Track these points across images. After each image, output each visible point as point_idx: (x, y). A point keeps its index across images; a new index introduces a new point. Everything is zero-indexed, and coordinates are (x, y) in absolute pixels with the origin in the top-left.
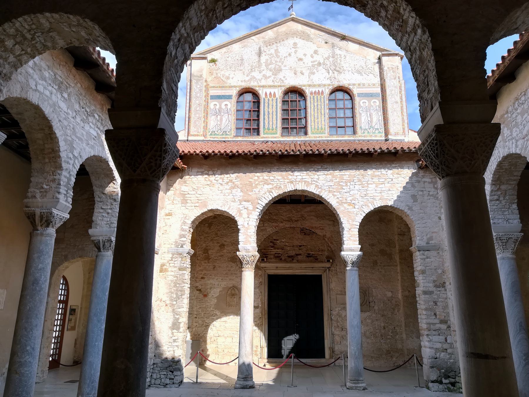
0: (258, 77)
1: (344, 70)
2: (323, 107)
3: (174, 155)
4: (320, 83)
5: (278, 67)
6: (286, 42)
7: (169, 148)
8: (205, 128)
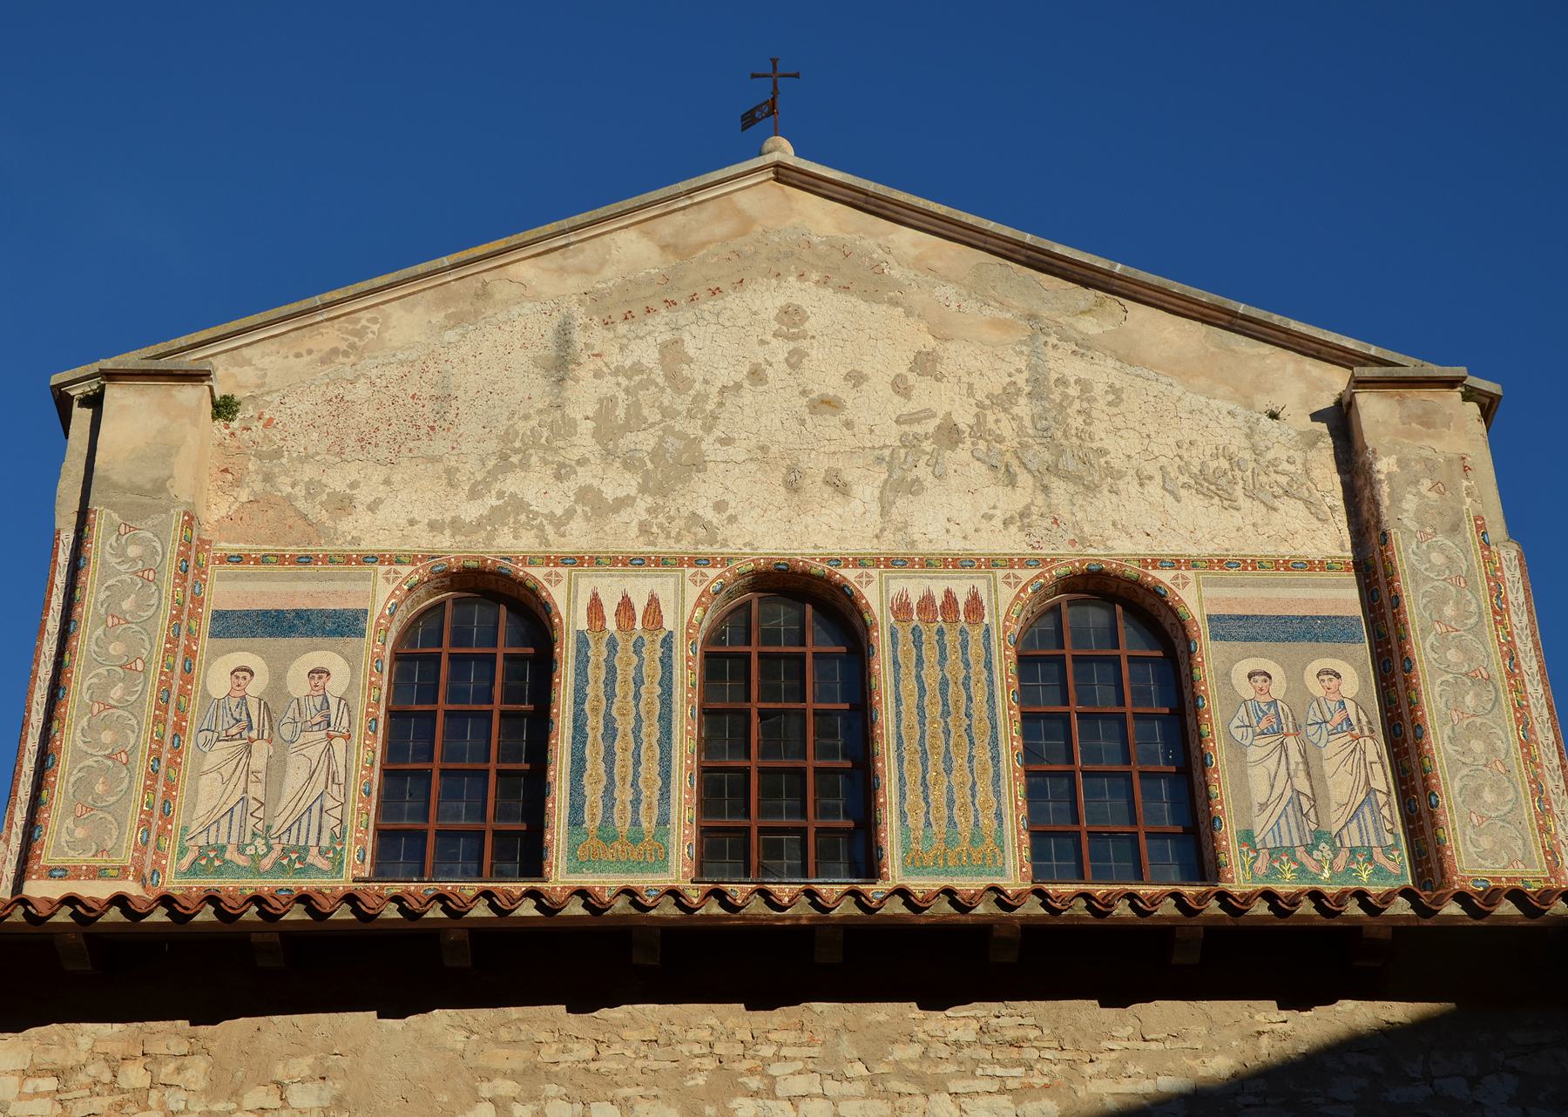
1: (1114, 474)
2: (979, 696)
4: (957, 546)
5: (680, 444)
6: (733, 302)
8: (156, 822)
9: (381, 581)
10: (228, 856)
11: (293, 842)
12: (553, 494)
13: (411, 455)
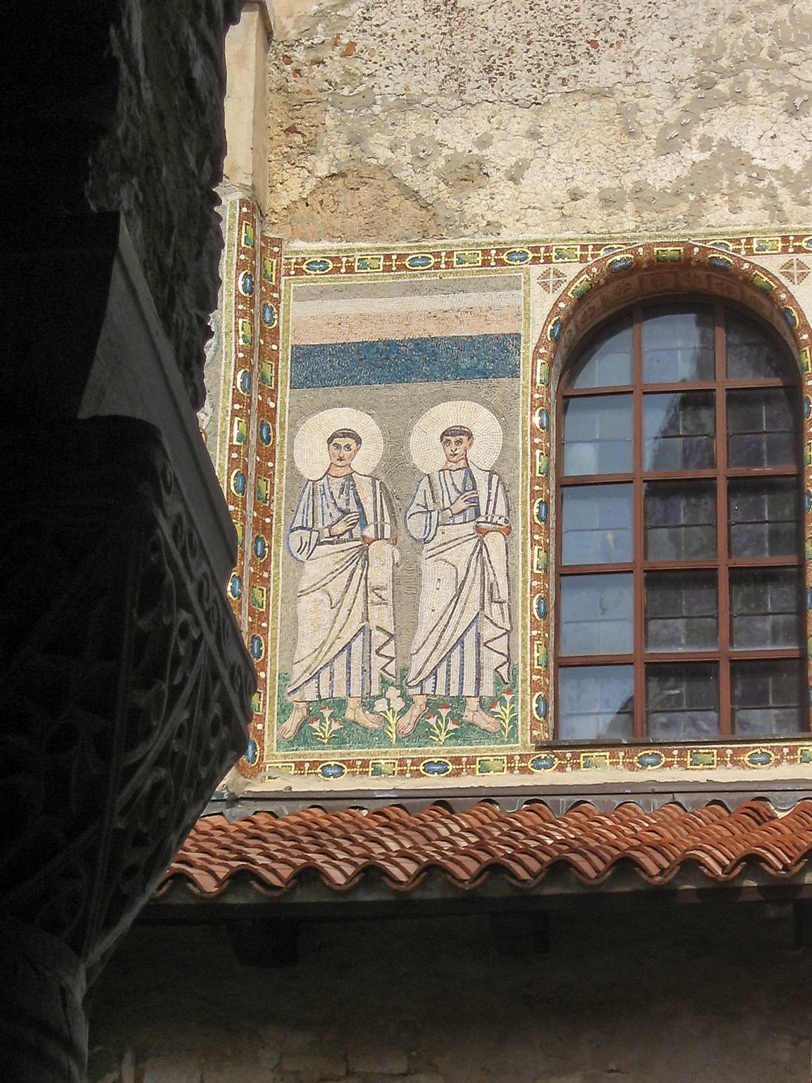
0: (762, 156)
3: (216, 709)
7: (184, 631)
9: (536, 289)
10: (349, 715)
11: (441, 691)
12: (783, 138)
13: (565, 89)
